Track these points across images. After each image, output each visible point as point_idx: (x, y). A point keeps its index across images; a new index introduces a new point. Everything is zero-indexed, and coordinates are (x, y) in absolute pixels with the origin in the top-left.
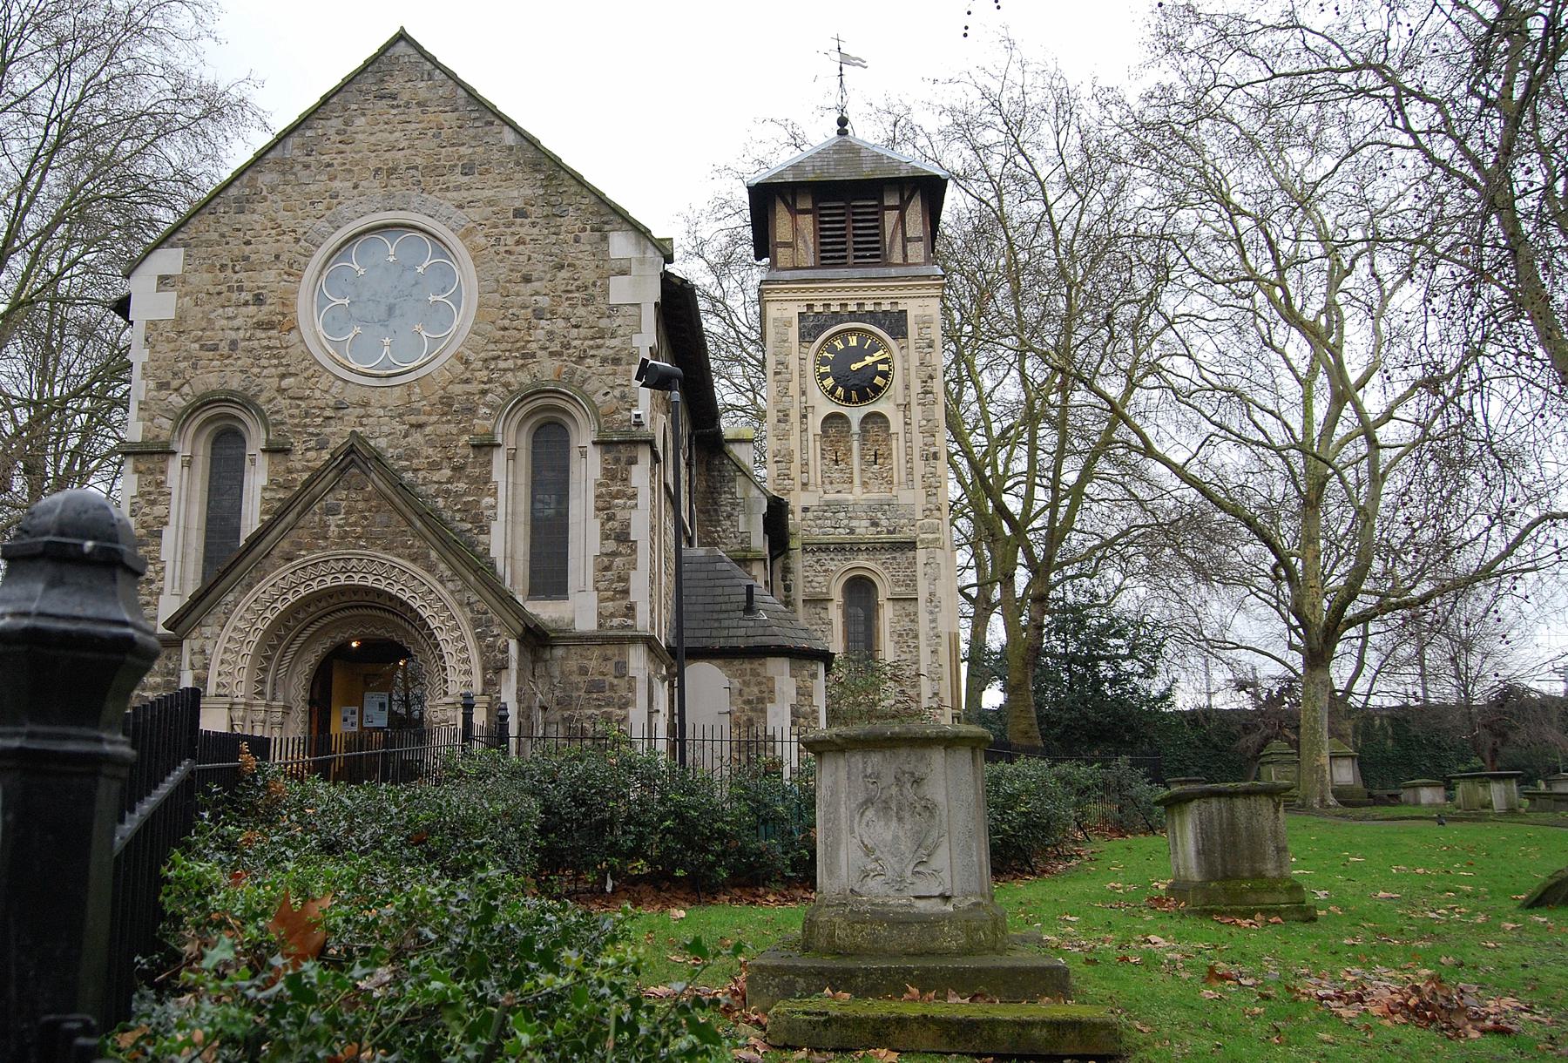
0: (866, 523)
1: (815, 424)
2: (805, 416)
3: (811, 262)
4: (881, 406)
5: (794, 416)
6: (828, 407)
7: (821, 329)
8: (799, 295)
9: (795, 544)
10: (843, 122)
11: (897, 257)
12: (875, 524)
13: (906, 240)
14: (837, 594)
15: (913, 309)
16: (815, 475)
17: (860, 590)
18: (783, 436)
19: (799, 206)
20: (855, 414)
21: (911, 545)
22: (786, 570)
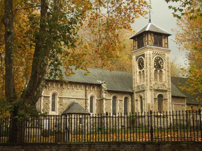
0: (141, 88)
1: (138, 73)
2: (136, 73)
3: (137, 48)
4: (143, 69)
5: (135, 73)
6: (138, 70)
7: (138, 58)
8: (134, 54)
9: (134, 92)
10: (150, 20)
11: (145, 45)
12: (142, 88)
13: (146, 41)
14: (139, 99)
15: (145, 53)
16: (138, 81)
17: (141, 97)
18: (134, 76)
19: (152, 35)
20: (141, 71)
21: (144, 91)
22: (134, 96)
